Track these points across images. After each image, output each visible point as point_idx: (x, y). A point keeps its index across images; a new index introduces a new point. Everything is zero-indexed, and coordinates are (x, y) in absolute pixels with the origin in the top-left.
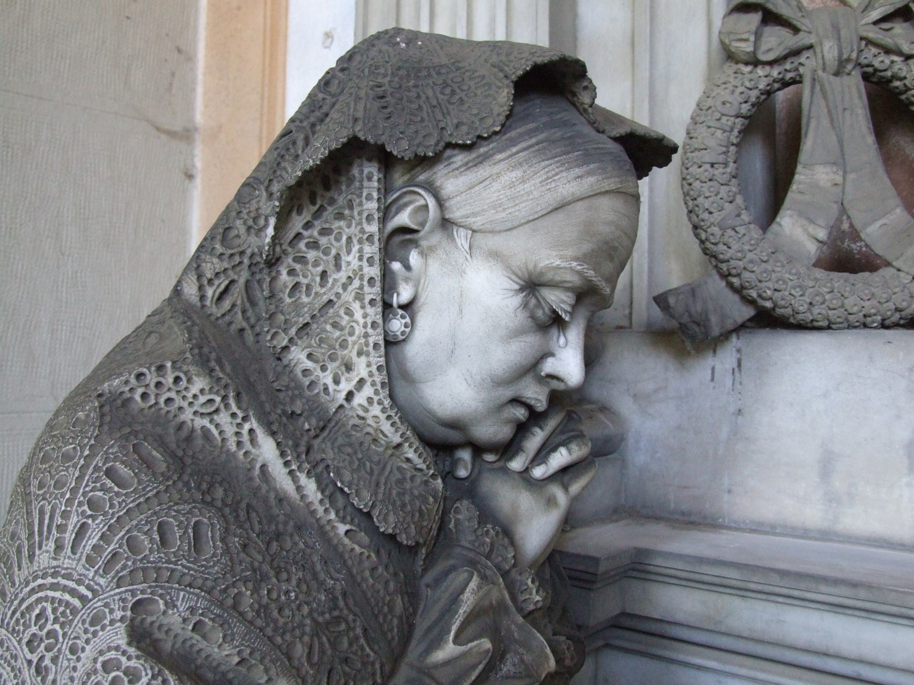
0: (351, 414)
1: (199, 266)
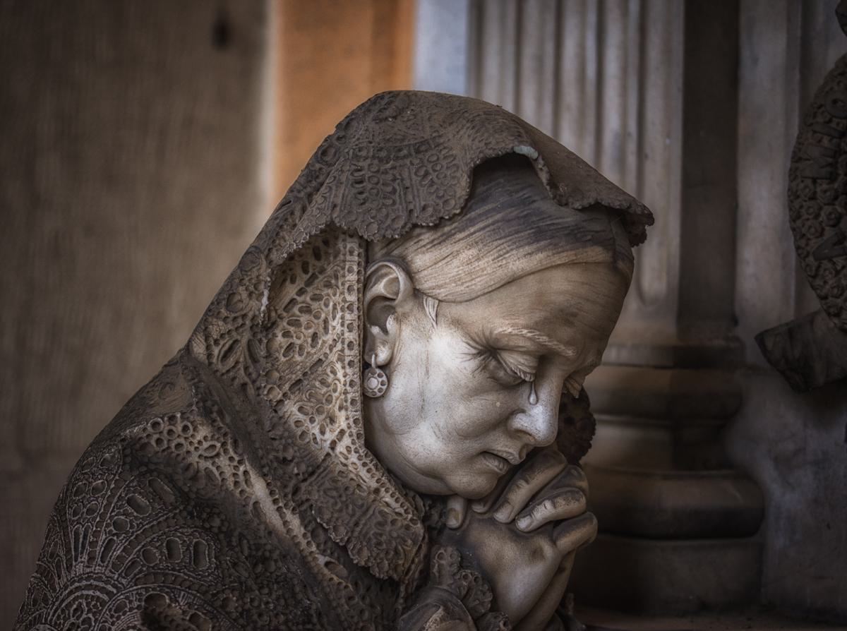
0: (336, 461)
1: (206, 328)
